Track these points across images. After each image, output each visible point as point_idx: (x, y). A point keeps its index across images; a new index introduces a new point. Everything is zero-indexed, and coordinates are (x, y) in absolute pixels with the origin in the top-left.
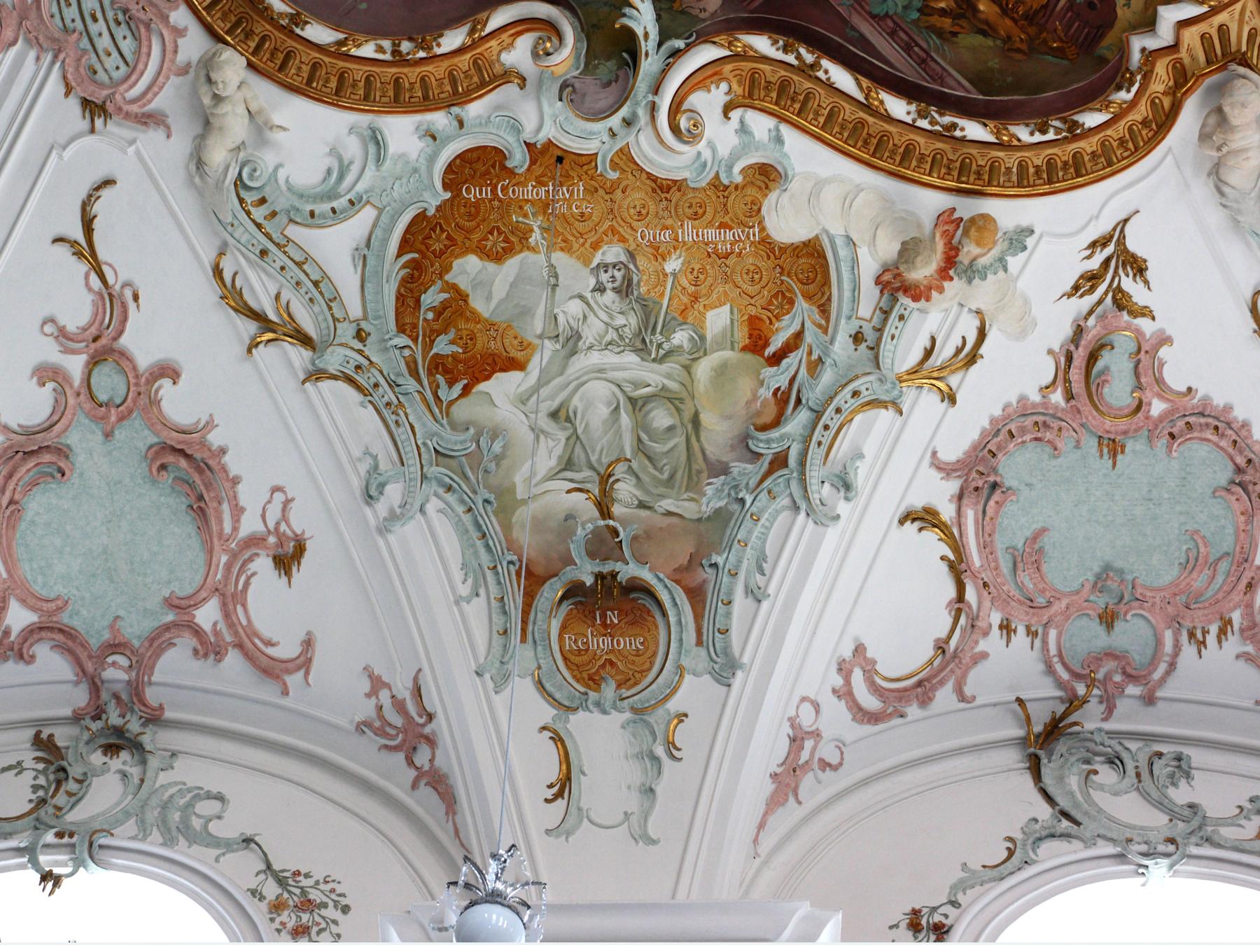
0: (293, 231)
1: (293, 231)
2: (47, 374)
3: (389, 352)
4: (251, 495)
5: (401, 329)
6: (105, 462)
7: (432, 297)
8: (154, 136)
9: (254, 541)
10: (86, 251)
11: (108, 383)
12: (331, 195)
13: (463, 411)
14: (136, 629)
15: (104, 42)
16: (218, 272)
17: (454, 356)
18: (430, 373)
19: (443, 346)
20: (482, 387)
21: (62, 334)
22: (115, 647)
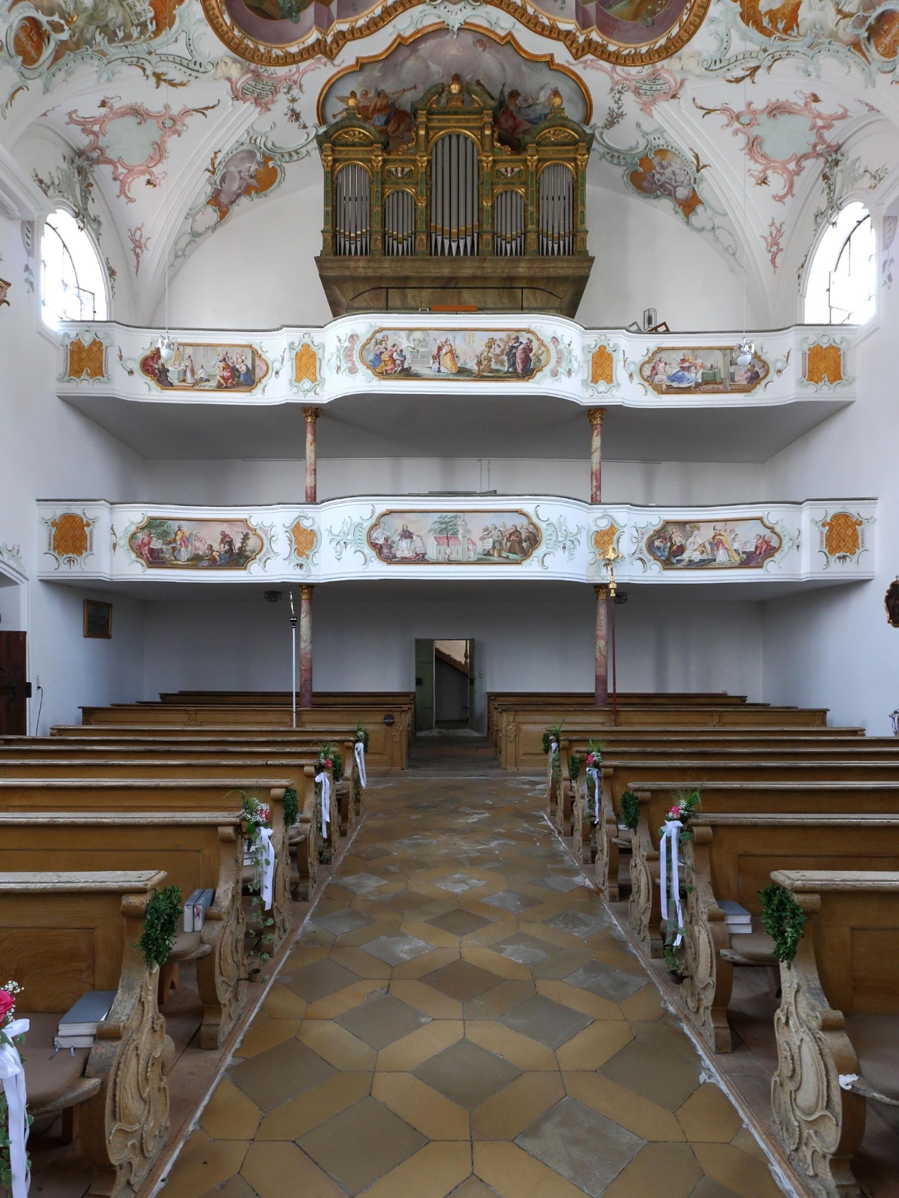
0: (727, 57)
1: (727, 57)
2: (736, 133)
3: (774, 44)
4: (793, 99)
5: (769, 36)
6: (765, 128)
7: (765, 22)
8: (687, 83)
9: (806, 104)
10: (709, 111)
11: (745, 119)
12: (722, 40)
13: (802, 31)
14: (813, 139)
15: (659, 87)
16: (730, 81)
17: (786, 23)
18: (787, 34)
19: (781, 26)
20: (799, 19)
21: (727, 125)
22: (815, 146)
